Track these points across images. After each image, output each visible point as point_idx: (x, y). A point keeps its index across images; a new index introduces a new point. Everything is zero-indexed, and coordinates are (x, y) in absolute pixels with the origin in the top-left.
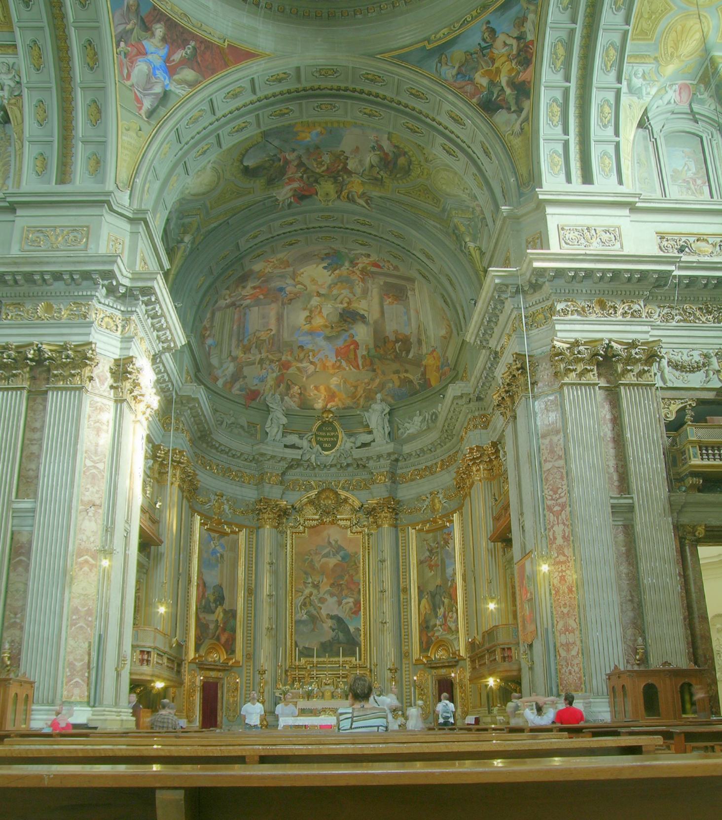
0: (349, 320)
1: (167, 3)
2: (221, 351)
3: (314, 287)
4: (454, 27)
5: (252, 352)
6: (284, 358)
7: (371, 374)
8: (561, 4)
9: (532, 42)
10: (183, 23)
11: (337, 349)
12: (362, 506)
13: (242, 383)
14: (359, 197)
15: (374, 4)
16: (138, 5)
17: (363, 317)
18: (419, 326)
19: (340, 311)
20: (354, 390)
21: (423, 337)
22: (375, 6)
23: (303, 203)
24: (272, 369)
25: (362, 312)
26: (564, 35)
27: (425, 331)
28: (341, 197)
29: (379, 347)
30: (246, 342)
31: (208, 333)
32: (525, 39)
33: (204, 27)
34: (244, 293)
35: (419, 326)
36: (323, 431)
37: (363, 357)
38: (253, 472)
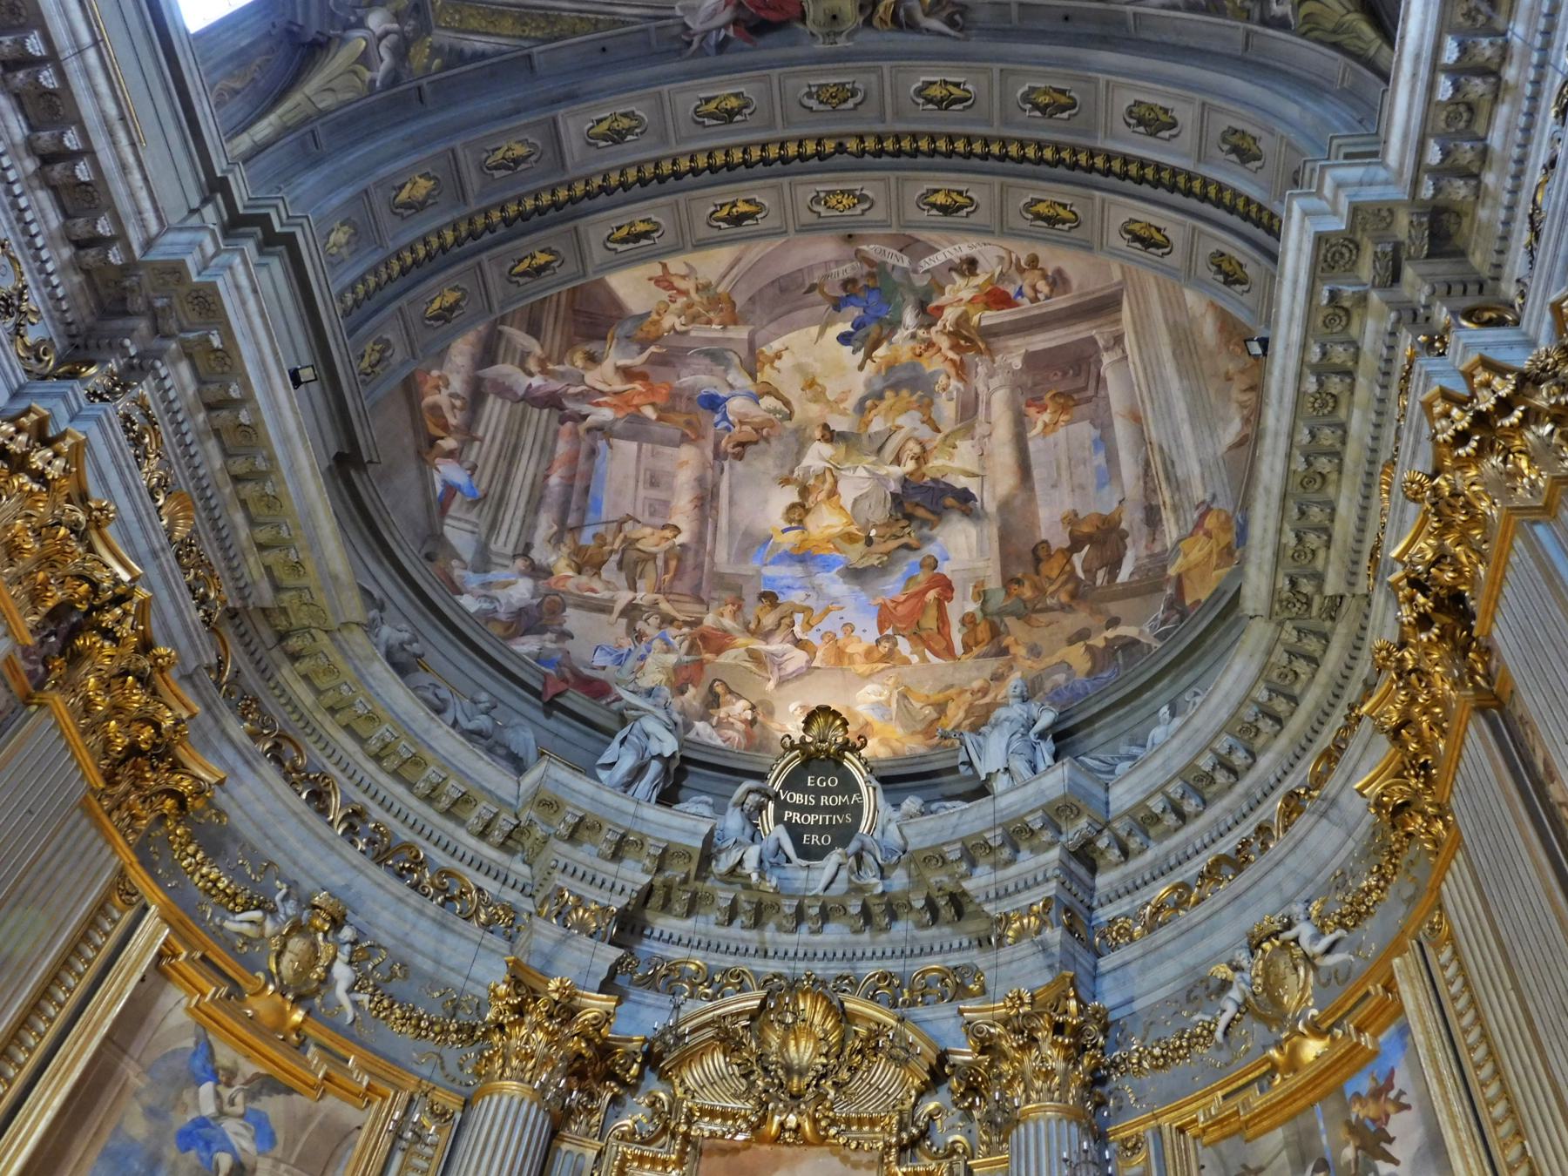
0: (921, 512)
2: (493, 526)
3: (814, 410)
5: (604, 574)
6: (709, 620)
7: (993, 665)
11: (883, 606)
12: (943, 1057)
13: (549, 645)
14: (927, 14)
17: (965, 497)
18: (1147, 464)
19: (894, 486)
20: (935, 715)
21: (1165, 495)
23: (761, 42)
24: (667, 643)
25: (961, 482)
27: (1169, 466)
28: (876, 22)
29: (1019, 582)
30: (586, 537)
31: (449, 443)
34: (593, 378)
35: (1147, 464)
36: (805, 790)
37: (968, 621)
38: (512, 896)
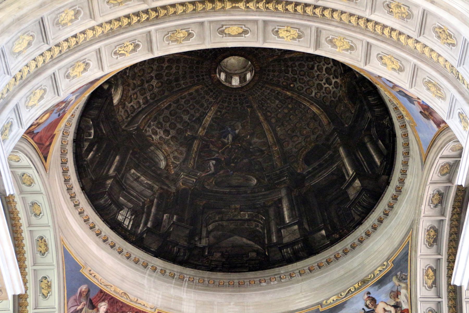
1: (111, 286)
4: (341, 295)
8: (426, 284)
9: (408, 310)
10: (123, 299)
15: (276, 275)
16: (89, 291)
22: (276, 277)
26: (433, 306)
32: (401, 307)
33: (140, 301)
